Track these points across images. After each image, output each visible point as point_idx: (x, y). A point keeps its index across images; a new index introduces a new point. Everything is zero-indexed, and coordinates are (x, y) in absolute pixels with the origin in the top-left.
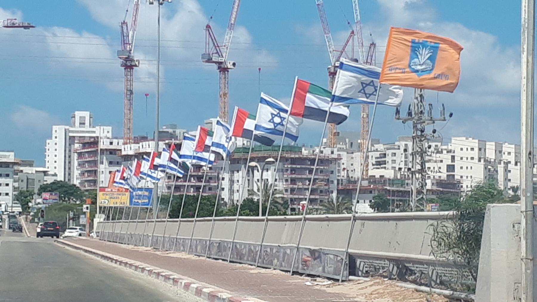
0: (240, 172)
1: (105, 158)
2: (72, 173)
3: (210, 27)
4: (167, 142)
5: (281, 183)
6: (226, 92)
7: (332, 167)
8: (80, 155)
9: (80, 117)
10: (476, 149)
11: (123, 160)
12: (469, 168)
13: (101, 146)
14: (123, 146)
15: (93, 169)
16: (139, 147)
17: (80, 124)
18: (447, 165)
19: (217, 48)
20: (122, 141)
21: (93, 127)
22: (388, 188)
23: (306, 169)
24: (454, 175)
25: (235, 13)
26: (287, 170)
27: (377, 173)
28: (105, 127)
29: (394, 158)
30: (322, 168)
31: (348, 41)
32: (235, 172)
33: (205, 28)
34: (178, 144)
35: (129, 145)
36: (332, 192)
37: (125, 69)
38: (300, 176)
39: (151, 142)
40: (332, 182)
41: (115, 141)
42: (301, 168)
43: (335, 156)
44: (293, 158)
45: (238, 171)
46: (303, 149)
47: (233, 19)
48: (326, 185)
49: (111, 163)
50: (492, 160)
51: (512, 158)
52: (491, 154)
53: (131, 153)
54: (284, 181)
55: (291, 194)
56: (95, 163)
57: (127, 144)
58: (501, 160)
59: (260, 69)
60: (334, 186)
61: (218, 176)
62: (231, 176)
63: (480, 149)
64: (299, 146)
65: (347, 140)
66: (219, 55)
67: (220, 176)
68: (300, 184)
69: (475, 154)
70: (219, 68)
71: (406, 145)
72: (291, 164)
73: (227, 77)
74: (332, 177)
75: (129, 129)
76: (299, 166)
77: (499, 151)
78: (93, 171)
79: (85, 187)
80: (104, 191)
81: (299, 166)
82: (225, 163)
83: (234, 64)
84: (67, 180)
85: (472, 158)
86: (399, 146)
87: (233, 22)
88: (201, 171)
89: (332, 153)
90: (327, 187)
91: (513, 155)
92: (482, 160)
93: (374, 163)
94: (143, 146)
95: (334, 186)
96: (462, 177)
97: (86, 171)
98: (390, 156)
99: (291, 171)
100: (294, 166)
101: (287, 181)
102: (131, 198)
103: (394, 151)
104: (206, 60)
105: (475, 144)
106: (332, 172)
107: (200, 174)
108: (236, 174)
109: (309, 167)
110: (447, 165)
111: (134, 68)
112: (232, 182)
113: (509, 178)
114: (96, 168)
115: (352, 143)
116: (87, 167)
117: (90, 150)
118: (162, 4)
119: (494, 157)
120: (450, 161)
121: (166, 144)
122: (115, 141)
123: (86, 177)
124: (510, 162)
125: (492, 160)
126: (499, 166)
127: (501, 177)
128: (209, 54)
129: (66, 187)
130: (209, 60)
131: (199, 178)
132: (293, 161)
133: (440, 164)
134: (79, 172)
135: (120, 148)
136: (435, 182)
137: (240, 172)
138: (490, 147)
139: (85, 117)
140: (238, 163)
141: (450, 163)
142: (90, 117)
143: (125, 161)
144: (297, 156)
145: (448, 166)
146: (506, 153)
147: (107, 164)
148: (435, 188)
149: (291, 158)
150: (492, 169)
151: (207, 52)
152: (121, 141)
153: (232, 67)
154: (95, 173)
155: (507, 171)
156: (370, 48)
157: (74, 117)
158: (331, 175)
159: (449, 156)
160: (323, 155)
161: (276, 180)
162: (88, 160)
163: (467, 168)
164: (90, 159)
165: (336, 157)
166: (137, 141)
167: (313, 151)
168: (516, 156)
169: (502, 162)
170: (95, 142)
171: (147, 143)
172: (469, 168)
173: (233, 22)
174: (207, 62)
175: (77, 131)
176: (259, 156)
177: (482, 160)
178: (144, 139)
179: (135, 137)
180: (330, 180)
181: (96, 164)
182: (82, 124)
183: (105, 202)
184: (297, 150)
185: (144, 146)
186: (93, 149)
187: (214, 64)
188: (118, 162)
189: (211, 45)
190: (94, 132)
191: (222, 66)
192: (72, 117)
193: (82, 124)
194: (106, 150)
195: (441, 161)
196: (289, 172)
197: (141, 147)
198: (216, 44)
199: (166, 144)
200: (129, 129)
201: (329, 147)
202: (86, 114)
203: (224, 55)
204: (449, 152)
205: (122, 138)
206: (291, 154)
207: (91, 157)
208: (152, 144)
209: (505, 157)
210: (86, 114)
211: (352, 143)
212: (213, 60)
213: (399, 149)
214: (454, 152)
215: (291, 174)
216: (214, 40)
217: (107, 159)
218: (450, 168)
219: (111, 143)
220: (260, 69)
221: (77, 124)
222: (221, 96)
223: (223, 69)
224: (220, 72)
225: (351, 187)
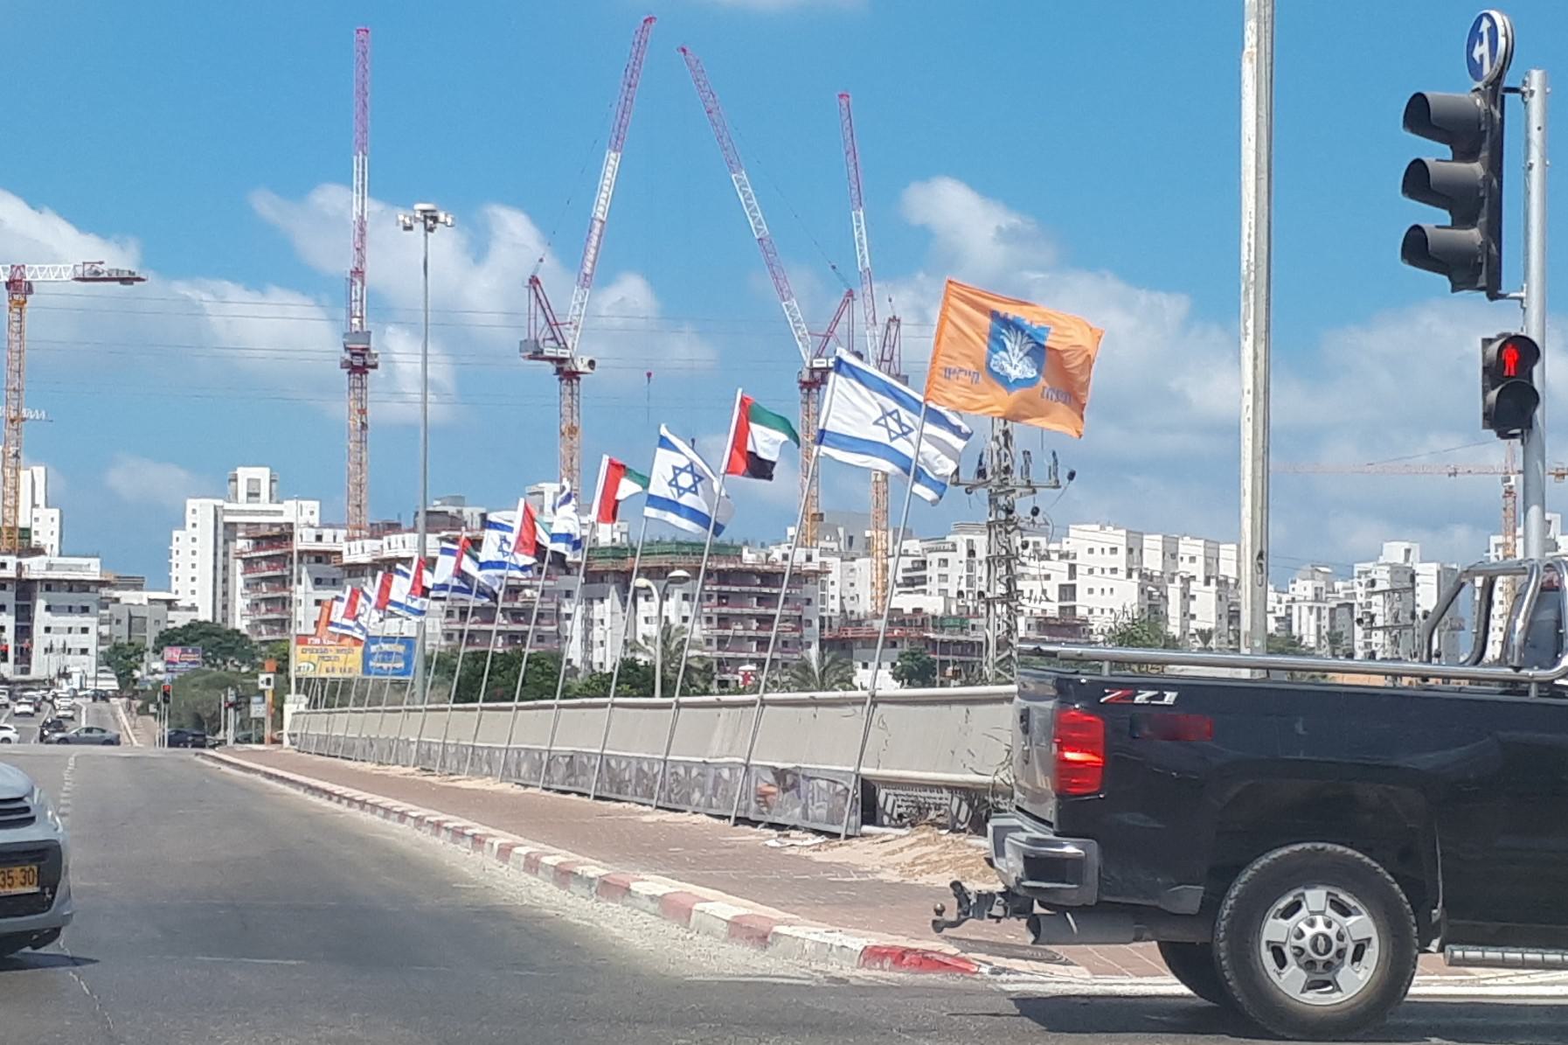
0: (606, 601)
1: (304, 570)
3: (538, 282)
5: (697, 627)
7: (809, 589)
8: (249, 563)
9: (249, 480)
10: (1122, 551)
11: (346, 575)
12: (1107, 591)
13: (298, 545)
14: (346, 545)
15: (278, 594)
16: (382, 546)
17: (249, 495)
19: (555, 328)
20: (344, 532)
21: (278, 502)
22: (932, 635)
23: (750, 594)
24: (1074, 608)
26: (709, 597)
27: (906, 602)
28: (305, 503)
29: (944, 571)
32: (596, 602)
33: (527, 283)
35: (359, 543)
36: (809, 645)
37: (349, 373)
38: (738, 611)
39: (407, 536)
40: (809, 623)
41: (327, 534)
42: (742, 593)
43: (814, 566)
44: (723, 570)
45: (602, 600)
46: (745, 551)
48: (794, 630)
51: (1198, 570)
52: (1153, 561)
53: (364, 559)
54: (703, 620)
55: (719, 649)
56: (284, 582)
57: (353, 539)
58: (1174, 574)
59: (649, 375)
60: (813, 633)
61: (558, 610)
62: (587, 610)
63: (1130, 551)
64: (735, 543)
65: (841, 531)
66: (559, 344)
67: (565, 610)
68: (740, 627)
69: (1120, 560)
70: (559, 371)
71: (970, 542)
72: (719, 584)
73: (576, 392)
74: (812, 614)
75: (359, 506)
77: (1171, 555)
78: (278, 598)
79: (260, 634)
80: (305, 643)
83: (592, 364)
84: (219, 620)
85: (1114, 570)
86: (954, 545)
87: (588, 271)
88: (521, 600)
89: (809, 559)
90: (797, 634)
91: (1200, 560)
92: (1135, 575)
94: (389, 544)
95: (813, 633)
96: (1091, 611)
98: (935, 564)
99: (720, 598)
100: (726, 588)
101: (709, 620)
102: (367, 657)
104: (530, 353)
105: (1119, 538)
106: (809, 601)
107: (518, 605)
108: (597, 606)
109: (757, 589)
111: (370, 370)
112: (588, 623)
113: (1192, 612)
114: (286, 594)
115: (851, 538)
117: (270, 553)
118: (431, 230)
119: (1160, 569)
120: (1067, 575)
122: (327, 534)
124: (1193, 578)
127: (1174, 609)
128: (536, 341)
129: (217, 636)
130: (537, 355)
131: (516, 615)
132: (724, 577)
133: (1046, 584)
134: (248, 601)
135: (338, 549)
136: (1033, 621)
137: (607, 602)
139: (258, 481)
140: (602, 581)
141: (1066, 581)
142: (272, 481)
143: (349, 576)
145: (1062, 587)
146: (1186, 559)
148: (1033, 635)
149: (719, 571)
151: (533, 338)
152: (342, 533)
153: (587, 370)
154: (284, 604)
155: (1187, 596)
156: (888, 328)
157: (236, 480)
158: (806, 607)
159: (1064, 564)
161: (685, 619)
164: (271, 573)
165: (818, 568)
166: (377, 532)
167: (768, 556)
168: (1207, 565)
169: (1177, 579)
170: (284, 535)
171: (400, 537)
172: (1107, 591)
173: (588, 271)
174: (530, 358)
175: (242, 509)
176: (649, 565)
177: (1135, 575)
178: (394, 527)
179: (372, 525)
180: (804, 618)
181: (284, 582)
182: (253, 495)
183: (308, 668)
185: (393, 545)
186: (278, 552)
187: (548, 363)
188: (334, 580)
189: (541, 320)
190: (280, 513)
191: (566, 367)
192: (230, 480)
193: (253, 495)
194: (308, 552)
195: (1048, 577)
196: (714, 601)
197: (386, 546)
198: (551, 319)
200: (359, 506)
201: (802, 546)
202: (263, 474)
203: (569, 345)
205: (341, 527)
206: (719, 562)
207: (275, 569)
208: (412, 539)
209: (1184, 567)
210: (263, 474)
211: (851, 538)
212: (546, 354)
213: (955, 550)
214: (1075, 557)
215: (720, 604)
216: (547, 311)
217: (309, 572)
218: (1068, 591)
219: (319, 538)
220: (649, 375)
221: (242, 495)
222: (563, 434)
223: (568, 374)
224: (561, 380)
225: (850, 635)
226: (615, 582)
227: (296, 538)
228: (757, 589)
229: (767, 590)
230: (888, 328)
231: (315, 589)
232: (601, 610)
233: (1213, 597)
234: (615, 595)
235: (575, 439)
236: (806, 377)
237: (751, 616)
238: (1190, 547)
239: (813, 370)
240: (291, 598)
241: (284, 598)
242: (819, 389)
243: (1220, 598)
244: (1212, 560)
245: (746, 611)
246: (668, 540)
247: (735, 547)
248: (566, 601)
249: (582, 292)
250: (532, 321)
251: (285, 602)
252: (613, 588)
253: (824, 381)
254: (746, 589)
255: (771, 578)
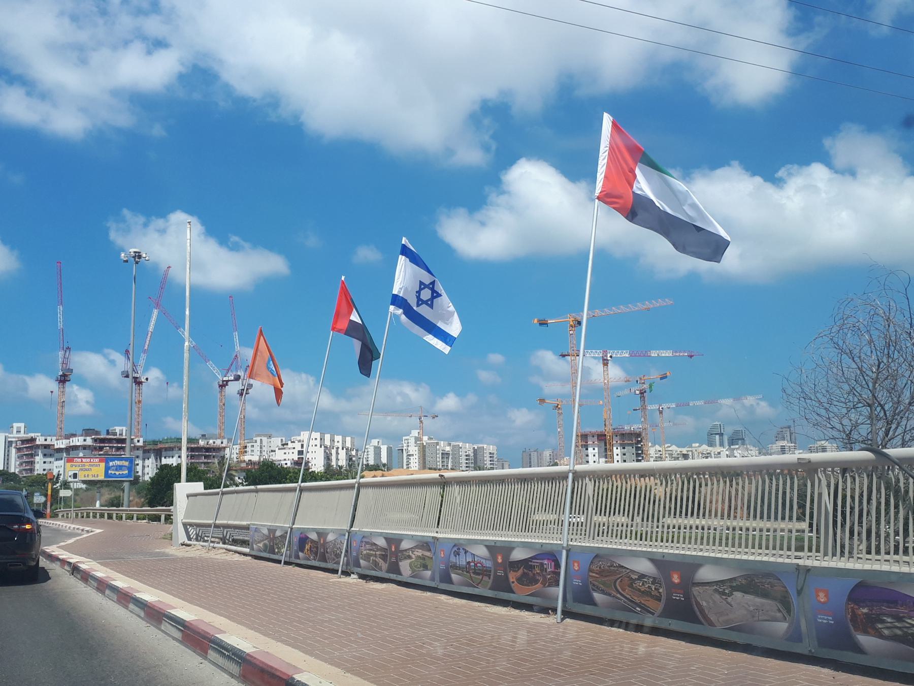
0: (150, 459)
2: (10, 463)
3: (128, 351)
4: (93, 437)
6: (140, 400)
8: (19, 450)
11: (56, 452)
12: (314, 452)
14: (56, 442)
15: (30, 460)
16: (70, 442)
18: (298, 451)
20: (55, 438)
23: (202, 455)
25: (148, 342)
29: (253, 449)
30: (214, 454)
31: (232, 363)
32: (146, 460)
33: (125, 352)
34: (102, 438)
35: (61, 441)
38: (197, 461)
39: (80, 438)
41: (49, 438)
42: (199, 455)
43: (223, 445)
45: (148, 459)
46: (200, 441)
47: (147, 346)
49: (45, 455)
50: (328, 446)
52: (327, 442)
53: (63, 446)
56: (32, 456)
62: (143, 463)
63: (321, 439)
64: (197, 438)
66: (135, 373)
69: (318, 442)
72: (191, 452)
75: (61, 428)
76: (196, 454)
77: (332, 440)
78: (30, 461)
79: (23, 474)
81: (196, 454)
82: (140, 453)
83: (147, 379)
84: (5, 469)
85: (316, 445)
89: (222, 443)
92: (323, 446)
93: (238, 452)
94: (73, 441)
97: (24, 462)
98: (250, 447)
99: (191, 457)
100: (193, 453)
103: (252, 444)
108: (147, 461)
109: (205, 454)
110: (298, 451)
111: (67, 382)
112: (144, 467)
114: (33, 460)
116: (25, 459)
117: (27, 445)
119: (329, 444)
120: (300, 447)
121: (92, 439)
122: (49, 438)
123: (24, 467)
125: (328, 446)
126: (333, 450)
127: (334, 458)
128: (128, 371)
129: (7, 475)
133: (293, 450)
134: (18, 463)
135: (53, 444)
136: (293, 462)
138: (327, 437)
140: (149, 452)
141: (300, 449)
143: (57, 453)
144: (196, 446)
147: (42, 456)
150: (329, 453)
151: (126, 370)
152: (54, 438)
153: (145, 381)
154: (32, 463)
155: (337, 453)
156: (246, 369)
159: (300, 444)
160: (216, 444)
162: (26, 453)
163: (312, 452)
164: (27, 453)
165: (224, 446)
166: (67, 437)
167: (208, 442)
168: (343, 443)
169: (335, 448)
171: (77, 438)
172: (314, 452)
173: (146, 348)
174: (125, 377)
176: (167, 446)
177: (323, 446)
178: (74, 435)
184: (195, 441)
185: (74, 441)
186: (30, 445)
188: (51, 455)
191: (138, 380)
194: (42, 445)
195: (294, 448)
197: (71, 441)
199: (92, 439)
200: (61, 428)
203: (139, 372)
204: (299, 441)
206: (191, 444)
207: (29, 451)
208: (81, 439)
209: (336, 444)
214: (303, 441)
218: (301, 453)
219: (46, 440)
222: (136, 403)
224: (136, 384)
226: (154, 453)
227: (37, 440)
228: (205, 454)
229: (208, 454)
230: (246, 369)
231: (44, 458)
232: (147, 462)
233: (345, 454)
234: (153, 457)
235: (140, 405)
236: (221, 383)
237: (202, 463)
238: (338, 438)
239: (223, 381)
240: (35, 461)
241: (32, 461)
242: (225, 387)
243: (347, 454)
244: (344, 442)
245: (200, 461)
246: (173, 438)
247: (197, 440)
248: (137, 459)
249: (144, 355)
250: (126, 365)
251: (32, 463)
252: (153, 455)
253: (227, 385)
254: (201, 453)
255: (208, 449)
